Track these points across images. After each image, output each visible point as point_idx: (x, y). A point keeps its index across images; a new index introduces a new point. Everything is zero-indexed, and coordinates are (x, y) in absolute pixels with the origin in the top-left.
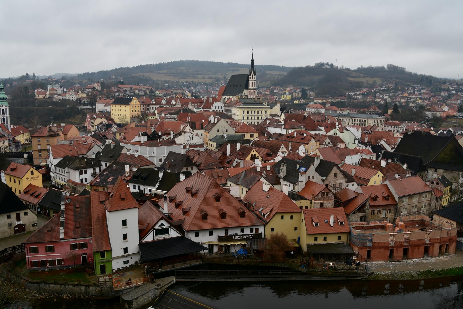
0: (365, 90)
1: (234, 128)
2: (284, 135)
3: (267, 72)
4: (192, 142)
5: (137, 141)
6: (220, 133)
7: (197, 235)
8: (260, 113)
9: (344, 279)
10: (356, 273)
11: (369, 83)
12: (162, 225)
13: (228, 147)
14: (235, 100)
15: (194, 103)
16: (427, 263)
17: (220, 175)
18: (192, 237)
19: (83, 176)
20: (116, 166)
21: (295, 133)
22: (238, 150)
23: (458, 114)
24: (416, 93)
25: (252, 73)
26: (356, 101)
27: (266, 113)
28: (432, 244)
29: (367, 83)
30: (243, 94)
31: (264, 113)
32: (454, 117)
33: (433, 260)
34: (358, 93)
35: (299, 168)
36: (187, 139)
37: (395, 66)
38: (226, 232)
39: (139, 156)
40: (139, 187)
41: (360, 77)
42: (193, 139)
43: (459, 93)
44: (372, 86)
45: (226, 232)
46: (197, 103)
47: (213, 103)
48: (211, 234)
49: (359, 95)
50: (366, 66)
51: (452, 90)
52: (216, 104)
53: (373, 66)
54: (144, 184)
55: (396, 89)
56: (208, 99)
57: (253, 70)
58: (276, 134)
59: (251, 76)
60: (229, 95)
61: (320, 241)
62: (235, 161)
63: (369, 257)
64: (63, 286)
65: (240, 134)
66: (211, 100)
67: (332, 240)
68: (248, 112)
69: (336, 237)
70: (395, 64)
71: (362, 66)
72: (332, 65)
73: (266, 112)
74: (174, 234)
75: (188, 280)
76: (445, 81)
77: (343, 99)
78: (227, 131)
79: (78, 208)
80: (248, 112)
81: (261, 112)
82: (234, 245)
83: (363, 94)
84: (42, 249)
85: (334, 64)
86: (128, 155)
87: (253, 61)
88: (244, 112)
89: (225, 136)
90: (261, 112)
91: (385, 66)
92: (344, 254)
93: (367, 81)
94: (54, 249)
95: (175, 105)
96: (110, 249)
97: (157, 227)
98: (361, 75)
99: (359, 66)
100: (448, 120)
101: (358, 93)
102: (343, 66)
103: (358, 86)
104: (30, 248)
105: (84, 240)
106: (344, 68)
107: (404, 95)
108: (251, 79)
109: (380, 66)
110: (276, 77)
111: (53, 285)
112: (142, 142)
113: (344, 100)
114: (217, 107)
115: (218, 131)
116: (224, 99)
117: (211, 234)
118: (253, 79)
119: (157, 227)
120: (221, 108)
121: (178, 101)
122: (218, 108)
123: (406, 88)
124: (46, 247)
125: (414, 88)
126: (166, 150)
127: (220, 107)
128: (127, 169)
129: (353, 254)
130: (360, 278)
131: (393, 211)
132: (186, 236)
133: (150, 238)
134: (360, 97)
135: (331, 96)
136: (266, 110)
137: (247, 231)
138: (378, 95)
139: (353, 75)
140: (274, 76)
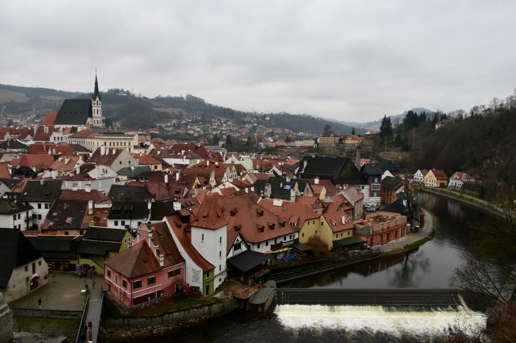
0: (174, 121)
2: (187, 165)
3: (42, 97)
4: (106, 175)
5: (48, 176)
6: (125, 165)
7: (259, 247)
8: (123, 144)
9: (371, 258)
10: (374, 254)
12: (238, 240)
13: (166, 177)
14: (83, 131)
15: (15, 134)
16: (397, 243)
17: (193, 203)
18: (255, 249)
19: (17, 222)
20: (67, 204)
21: (208, 162)
22: (177, 179)
23: (286, 144)
24: (224, 125)
25: (97, 99)
26: (169, 133)
27: (130, 143)
28: (398, 229)
29: (173, 114)
31: (127, 144)
32: (282, 147)
33: (400, 240)
34: (169, 124)
35: (283, 186)
36: (101, 173)
37: (194, 97)
38: (276, 242)
39: (92, 191)
40: (123, 223)
41: (162, 107)
42: (107, 173)
43: (261, 126)
44: (180, 117)
45: (276, 242)
47: (50, 133)
48: (267, 245)
49: (170, 126)
50: (164, 95)
51: (254, 122)
52: (55, 135)
53: (171, 96)
54: (131, 218)
55: (205, 122)
57: (98, 95)
58: (175, 165)
59: (96, 102)
60: (65, 124)
61: (340, 238)
63: (372, 244)
64: (187, 312)
65: (145, 166)
66: (46, 129)
67: (345, 235)
68: (110, 144)
69: (347, 232)
70: (194, 95)
71: (160, 95)
72: (128, 92)
73: (130, 143)
74: (244, 248)
75: (283, 281)
76: (245, 115)
77: (155, 131)
78: (130, 162)
79: (161, 235)
80: (110, 144)
81: (125, 143)
82: (279, 253)
83: (174, 126)
84: (144, 283)
85: (131, 92)
86: (74, 191)
87: (96, 84)
88: (105, 143)
89: (133, 168)
90: (125, 143)
91: (185, 97)
92: (359, 243)
93: (173, 112)
94: (155, 280)
96: (213, 267)
97: (235, 243)
98: (164, 105)
99: (157, 95)
100: (279, 149)
101: (169, 124)
102: (140, 95)
103: (166, 117)
104: (134, 283)
105: (172, 268)
106: (142, 96)
107: (214, 127)
108: (96, 105)
109: (179, 96)
110: (58, 103)
111: (177, 314)
113: (157, 132)
114: (56, 139)
115: (121, 163)
116: (58, 129)
117: (267, 245)
118: (99, 106)
119: (235, 243)
120: (62, 140)
122: (58, 140)
123: (213, 120)
124: (148, 279)
125: (220, 120)
126: (100, 185)
127: (60, 139)
128: (90, 205)
129: (363, 242)
130: (378, 256)
131: (351, 214)
132: (252, 249)
133: (231, 255)
134: (171, 129)
135: (141, 128)
136: (130, 141)
137: (288, 239)
138: (189, 127)
139: (155, 105)
140: (54, 102)
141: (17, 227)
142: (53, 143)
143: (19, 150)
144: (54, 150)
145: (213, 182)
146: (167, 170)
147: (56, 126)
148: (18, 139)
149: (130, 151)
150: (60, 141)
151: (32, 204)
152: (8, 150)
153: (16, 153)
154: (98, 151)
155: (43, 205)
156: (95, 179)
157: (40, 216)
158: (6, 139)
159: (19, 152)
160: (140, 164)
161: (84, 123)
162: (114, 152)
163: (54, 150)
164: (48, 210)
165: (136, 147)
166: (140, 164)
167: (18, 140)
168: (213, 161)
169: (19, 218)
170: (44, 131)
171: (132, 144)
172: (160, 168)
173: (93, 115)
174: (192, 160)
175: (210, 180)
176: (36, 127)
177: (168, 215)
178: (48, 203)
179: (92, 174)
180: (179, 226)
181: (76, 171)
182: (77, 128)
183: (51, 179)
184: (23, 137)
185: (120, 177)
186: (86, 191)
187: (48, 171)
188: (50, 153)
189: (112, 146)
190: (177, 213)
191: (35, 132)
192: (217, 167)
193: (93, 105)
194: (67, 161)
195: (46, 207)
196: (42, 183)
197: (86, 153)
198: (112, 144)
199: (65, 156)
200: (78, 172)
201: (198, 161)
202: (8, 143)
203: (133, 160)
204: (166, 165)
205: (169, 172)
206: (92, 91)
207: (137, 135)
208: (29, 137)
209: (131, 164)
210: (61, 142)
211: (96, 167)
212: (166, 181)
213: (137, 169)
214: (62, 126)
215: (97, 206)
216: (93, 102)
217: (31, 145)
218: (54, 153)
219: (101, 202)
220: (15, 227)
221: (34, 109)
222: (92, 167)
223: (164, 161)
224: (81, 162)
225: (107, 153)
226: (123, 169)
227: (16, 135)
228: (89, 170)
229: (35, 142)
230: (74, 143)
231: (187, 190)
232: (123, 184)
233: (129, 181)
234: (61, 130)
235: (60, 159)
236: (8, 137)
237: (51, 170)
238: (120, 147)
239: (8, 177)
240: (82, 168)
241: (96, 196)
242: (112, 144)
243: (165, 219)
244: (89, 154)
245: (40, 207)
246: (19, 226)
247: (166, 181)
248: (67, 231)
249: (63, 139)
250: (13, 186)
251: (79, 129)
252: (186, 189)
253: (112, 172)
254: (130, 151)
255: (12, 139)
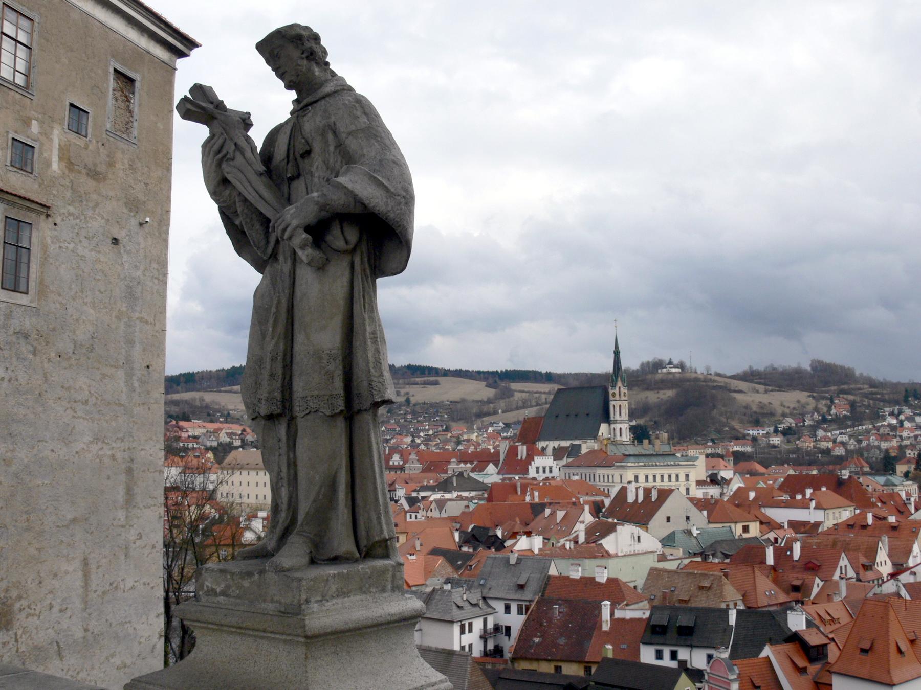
1: (705, 513)
2: (817, 525)
4: (639, 548)
6: (678, 525)
8: (673, 478)
11: (787, 404)
14: (592, 452)
15: (465, 462)
24: (907, 424)
25: (619, 384)
27: (687, 476)
30: (600, 434)
31: (682, 478)
39: (608, 579)
40: (674, 656)
42: (639, 541)
46: (471, 463)
52: (538, 461)
56: (513, 451)
60: (556, 439)
62: (815, 585)
66: (522, 450)
68: (647, 477)
71: (750, 367)
73: (687, 476)
77: (743, 445)
78: (688, 518)
80: (647, 477)
81: (677, 476)
85: (688, 364)
86: (574, 580)
87: (617, 353)
88: (636, 478)
89: (695, 532)
90: (677, 476)
95: (402, 468)
98: (761, 388)
102: (708, 368)
112: (536, 551)
113: (749, 449)
114: (541, 470)
115: (668, 519)
116: (544, 449)
118: (623, 398)
120: (551, 471)
121: (413, 456)
122: (544, 472)
127: (547, 470)
136: (687, 470)
138: (820, 433)
141: (467, 649)
142: (534, 479)
143: (473, 494)
144: (536, 494)
145: (884, 565)
146: (771, 536)
147: (540, 444)
148: (473, 470)
149: (688, 493)
150: (548, 474)
151: (493, 603)
152: (455, 494)
153: (466, 499)
154: (623, 491)
155: (514, 608)
156: (616, 556)
157: (508, 629)
158: (450, 472)
159: (472, 498)
160: (709, 522)
161: (595, 436)
162: (654, 495)
163: (536, 494)
164: (523, 618)
165: (699, 483)
166: (709, 522)
167: (471, 475)
168: (882, 513)
169: (470, 631)
170: (517, 455)
171: (693, 478)
172: (755, 529)
173: (612, 418)
174: (830, 512)
175: (878, 560)
176: (504, 447)
177: (771, 642)
178: (524, 604)
179: (608, 543)
180: (802, 671)
181: (577, 536)
182: (580, 445)
183: (529, 553)
184: (480, 468)
185: (668, 551)
186: (597, 579)
187: (524, 537)
188: (528, 499)
189: (651, 483)
190: (795, 638)
191: (502, 458)
192: (894, 528)
193: (611, 398)
194: (560, 514)
195: (520, 612)
196: (513, 561)
197: (598, 498)
198: (651, 479)
199: (557, 507)
200: (582, 539)
201: (847, 514)
202: (455, 479)
203: (693, 511)
204: (768, 524)
205: (776, 539)
206: (609, 367)
207: (702, 458)
208: (491, 468)
209: (691, 523)
210: (550, 476)
211: (619, 528)
212: (770, 561)
213: (703, 532)
214: (551, 445)
215: (618, 614)
216: (611, 392)
217: (495, 485)
218: (537, 500)
219: (627, 605)
220: (463, 648)
221: (500, 411)
222: (611, 529)
223: (764, 515)
224: (588, 518)
225: (641, 498)
226: (673, 533)
227: (469, 465)
228: (603, 536)
229: (501, 477)
230: (576, 478)
231: (821, 584)
232: (671, 566)
233: (686, 561)
234: (549, 451)
235: (548, 511)
236: (454, 467)
237: (528, 534)
238: (666, 485)
239: (453, 547)
240: (589, 531)
241: (615, 590)
242: (651, 479)
243: (766, 651)
244: (602, 501)
245: (507, 609)
246: (470, 646)
247: (770, 561)
248: (559, 664)
249: (553, 469)
250: (459, 567)
251: (584, 450)
252: (817, 580)
253: (650, 542)
254: (688, 493)
255: (461, 474)
